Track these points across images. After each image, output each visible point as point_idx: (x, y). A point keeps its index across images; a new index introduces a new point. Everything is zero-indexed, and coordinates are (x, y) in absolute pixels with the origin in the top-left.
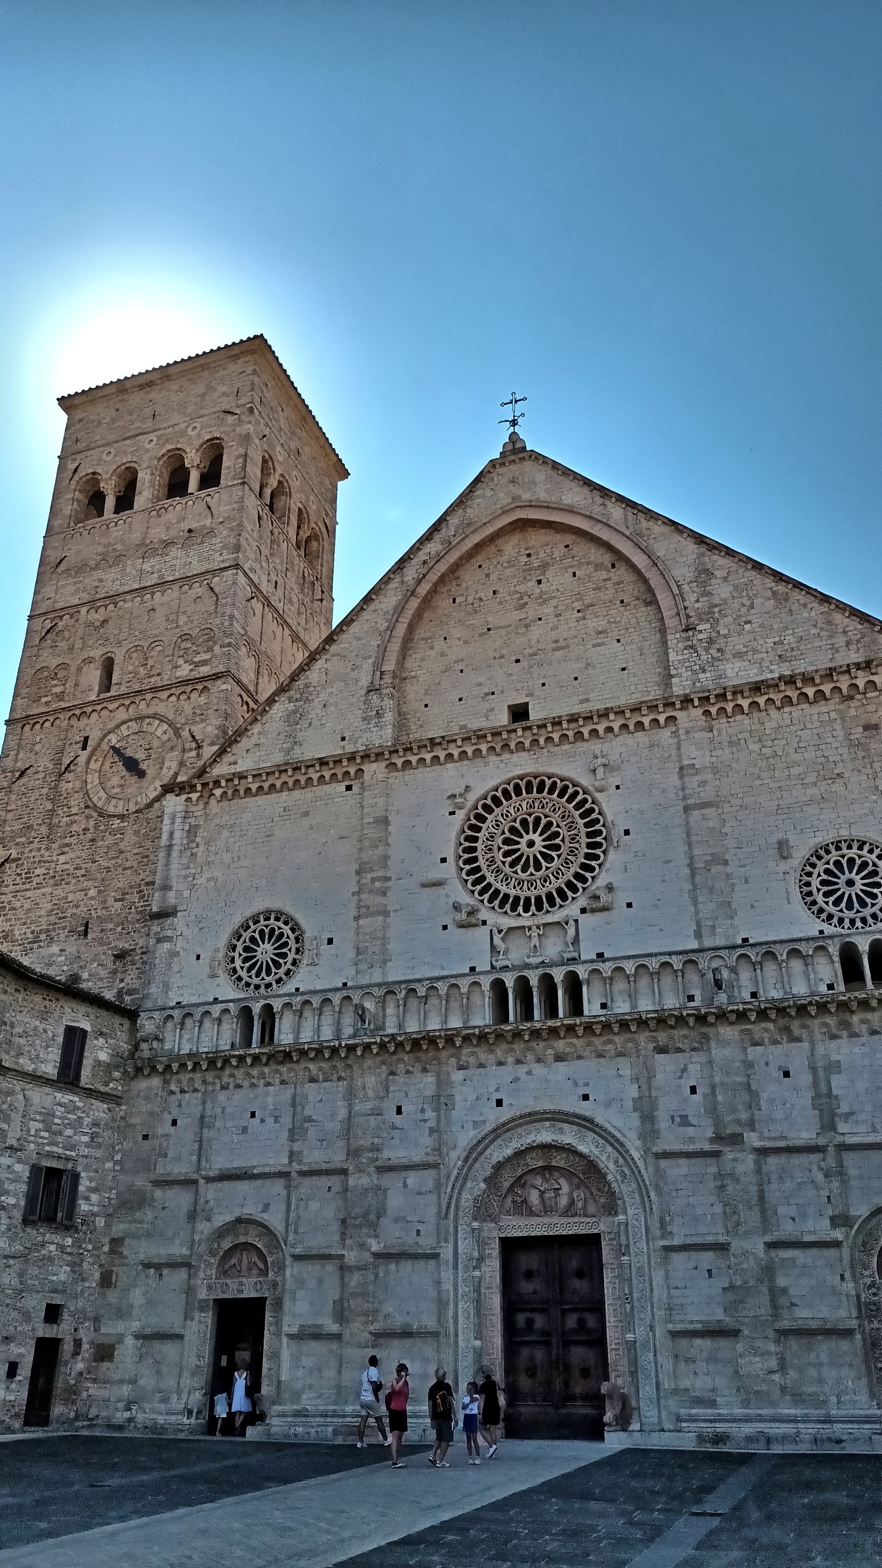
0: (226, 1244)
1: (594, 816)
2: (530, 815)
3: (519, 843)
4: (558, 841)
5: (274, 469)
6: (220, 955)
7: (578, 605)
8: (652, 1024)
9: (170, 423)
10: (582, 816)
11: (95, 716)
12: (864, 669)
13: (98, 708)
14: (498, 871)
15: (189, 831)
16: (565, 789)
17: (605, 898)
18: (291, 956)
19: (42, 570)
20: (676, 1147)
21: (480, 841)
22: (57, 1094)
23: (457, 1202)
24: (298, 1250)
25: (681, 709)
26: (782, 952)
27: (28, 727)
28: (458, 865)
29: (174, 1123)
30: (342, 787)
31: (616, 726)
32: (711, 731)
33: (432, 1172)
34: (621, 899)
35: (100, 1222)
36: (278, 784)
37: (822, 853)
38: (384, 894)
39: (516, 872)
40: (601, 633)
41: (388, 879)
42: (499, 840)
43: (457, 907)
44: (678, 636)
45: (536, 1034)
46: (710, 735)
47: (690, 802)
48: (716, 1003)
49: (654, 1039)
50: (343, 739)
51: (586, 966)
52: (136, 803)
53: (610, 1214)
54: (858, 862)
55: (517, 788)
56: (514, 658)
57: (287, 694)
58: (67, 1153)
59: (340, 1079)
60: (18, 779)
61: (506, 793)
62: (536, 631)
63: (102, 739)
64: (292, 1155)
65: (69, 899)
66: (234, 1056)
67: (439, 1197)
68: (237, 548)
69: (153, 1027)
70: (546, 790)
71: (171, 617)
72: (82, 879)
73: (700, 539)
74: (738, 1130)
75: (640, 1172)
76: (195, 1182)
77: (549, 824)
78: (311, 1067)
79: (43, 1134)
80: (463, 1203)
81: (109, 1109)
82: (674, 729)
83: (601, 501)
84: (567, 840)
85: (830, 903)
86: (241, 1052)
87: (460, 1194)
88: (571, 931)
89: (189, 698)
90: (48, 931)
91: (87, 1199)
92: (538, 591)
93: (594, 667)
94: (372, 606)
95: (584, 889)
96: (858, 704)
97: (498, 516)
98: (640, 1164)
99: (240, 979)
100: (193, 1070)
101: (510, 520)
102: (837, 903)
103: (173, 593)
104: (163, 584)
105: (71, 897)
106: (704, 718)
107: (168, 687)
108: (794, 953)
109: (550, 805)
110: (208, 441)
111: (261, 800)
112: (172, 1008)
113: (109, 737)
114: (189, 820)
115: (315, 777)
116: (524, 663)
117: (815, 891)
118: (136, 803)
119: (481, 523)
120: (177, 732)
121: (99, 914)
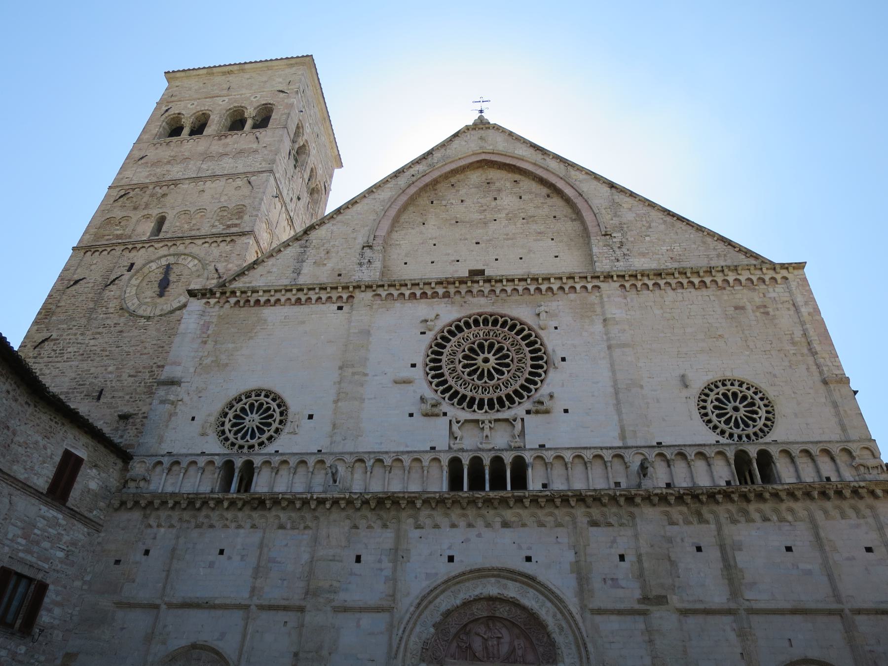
1: (537, 346)
2: (486, 340)
3: (475, 359)
4: (507, 361)
5: (303, 134)
6: (212, 419)
7: (523, 215)
8: (590, 500)
9: (239, 93)
10: (528, 345)
12: (732, 271)
13: (147, 245)
14: (459, 378)
17: (548, 404)
18: (275, 426)
19: (127, 161)
20: (610, 606)
21: (445, 355)
22: (42, 507)
23: (406, 645)
25: (603, 281)
26: (691, 453)
27: (89, 253)
28: (425, 370)
29: (147, 552)
30: (335, 307)
31: (555, 287)
32: (626, 298)
33: (385, 616)
34: (557, 407)
35: (58, 635)
36: (283, 299)
37: (713, 387)
38: (362, 385)
39: (473, 380)
40: (540, 233)
41: (366, 375)
42: (460, 356)
43: (423, 399)
44: (599, 238)
45: (488, 502)
46: (625, 301)
47: (613, 342)
48: (643, 487)
49: (589, 515)
51: (532, 452)
53: (548, 663)
54: (740, 395)
56: (474, 241)
57: (300, 242)
58: (40, 563)
59: (306, 528)
60: (72, 286)
62: (493, 226)
63: (144, 265)
64: (253, 590)
65: (91, 372)
66: (213, 499)
67: (390, 638)
68: (273, 161)
69: (142, 469)
70: (499, 325)
71: (218, 196)
72: (105, 358)
73: (612, 185)
74: (663, 593)
75: (577, 624)
76: (156, 607)
77: (501, 349)
78: (282, 515)
79: (20, 540)
80: (411, 644)
81: (89, 534)
82: (598, 294)
83: (543, 157)
84: (515, 360)
85: (722, 422)
86: (220, 496)
87: (409, 636)
89: (219, 245)
90: (67, 393)
91: (50, 611)
93: (534, 253)
94: (372, 196)
95: (528, 397)
96: (729, 293)
97: (469, 156)
98: (578, 617)
99: (227, 439)
100: (173, 508)
101: (478, 159)
102: (727, 422)
103: (222, 182)
104: (214, 177)
105: (93, 370)
106: (619, 289)
108: (700, 455)
109: (502, 335)
110: (263, 105)
112: (162, 456)
113: (151, 265)
114: (205, 318)
115: (314, 298)
117: (710, 413)
119: (457, 158)
120: (204, 266)
121: (114, 385)
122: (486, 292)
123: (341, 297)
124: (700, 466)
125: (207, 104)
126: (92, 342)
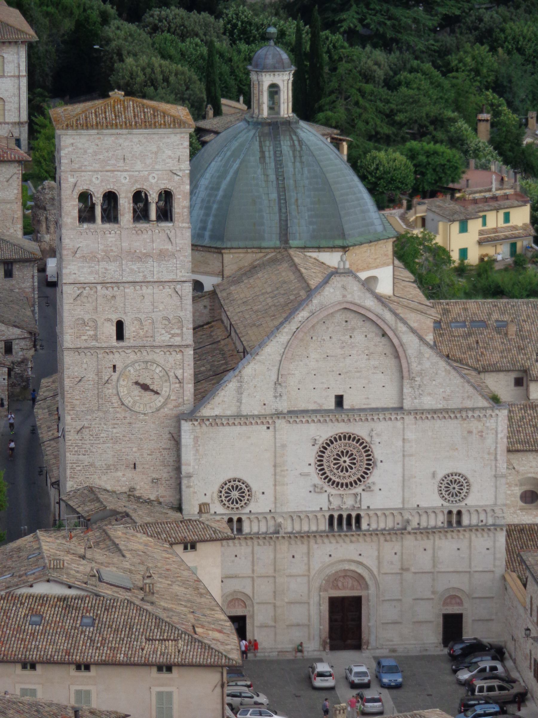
0: (229, 599)
4: (355, 461)
7: (366, 352)
11: (117, 355)
14: (331, 471)
15: (194, 438)
16: (359, 440)
17: (373, 488)
18: (247, 497)
20: (388, 571)
24: (258, 601)
26: (429, 511)
30: (265, 427)
41: (287, 470)
43: (315, 486)
50: (265, 404)
52: (150, 407)
55: (340, 437)
61: (335, 438)
64: (253, 571)
67: (309, 585)
77: (352, 454)
88: (359, 498)
92: (350, 341)
98: (377, 576)
99: (224, 504)
105: (123, 450)
107: (160, 347)
111: (227, 428)
116: (342, 376)
118: (150, 407)
122: (346, 420)
123: (268, 422)
124: (432, 516)
125: (111, 180)
126: (115, 431)
